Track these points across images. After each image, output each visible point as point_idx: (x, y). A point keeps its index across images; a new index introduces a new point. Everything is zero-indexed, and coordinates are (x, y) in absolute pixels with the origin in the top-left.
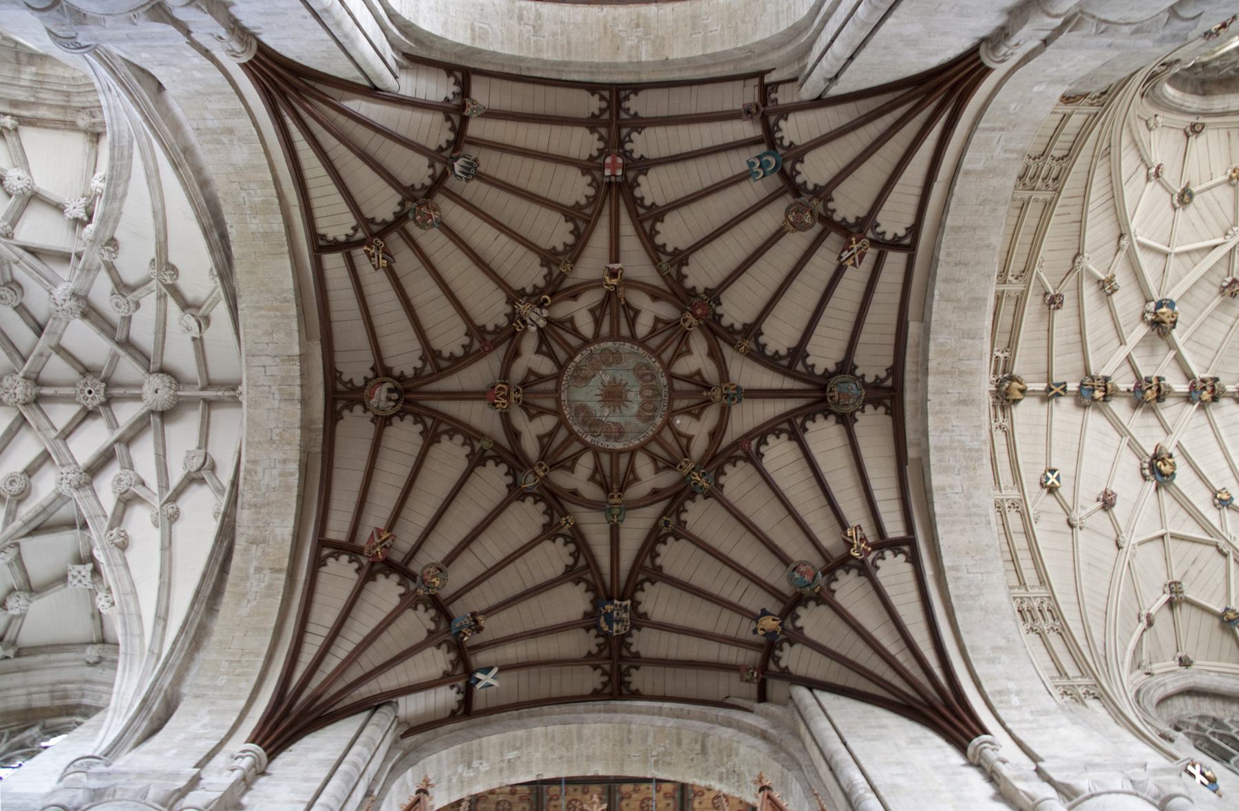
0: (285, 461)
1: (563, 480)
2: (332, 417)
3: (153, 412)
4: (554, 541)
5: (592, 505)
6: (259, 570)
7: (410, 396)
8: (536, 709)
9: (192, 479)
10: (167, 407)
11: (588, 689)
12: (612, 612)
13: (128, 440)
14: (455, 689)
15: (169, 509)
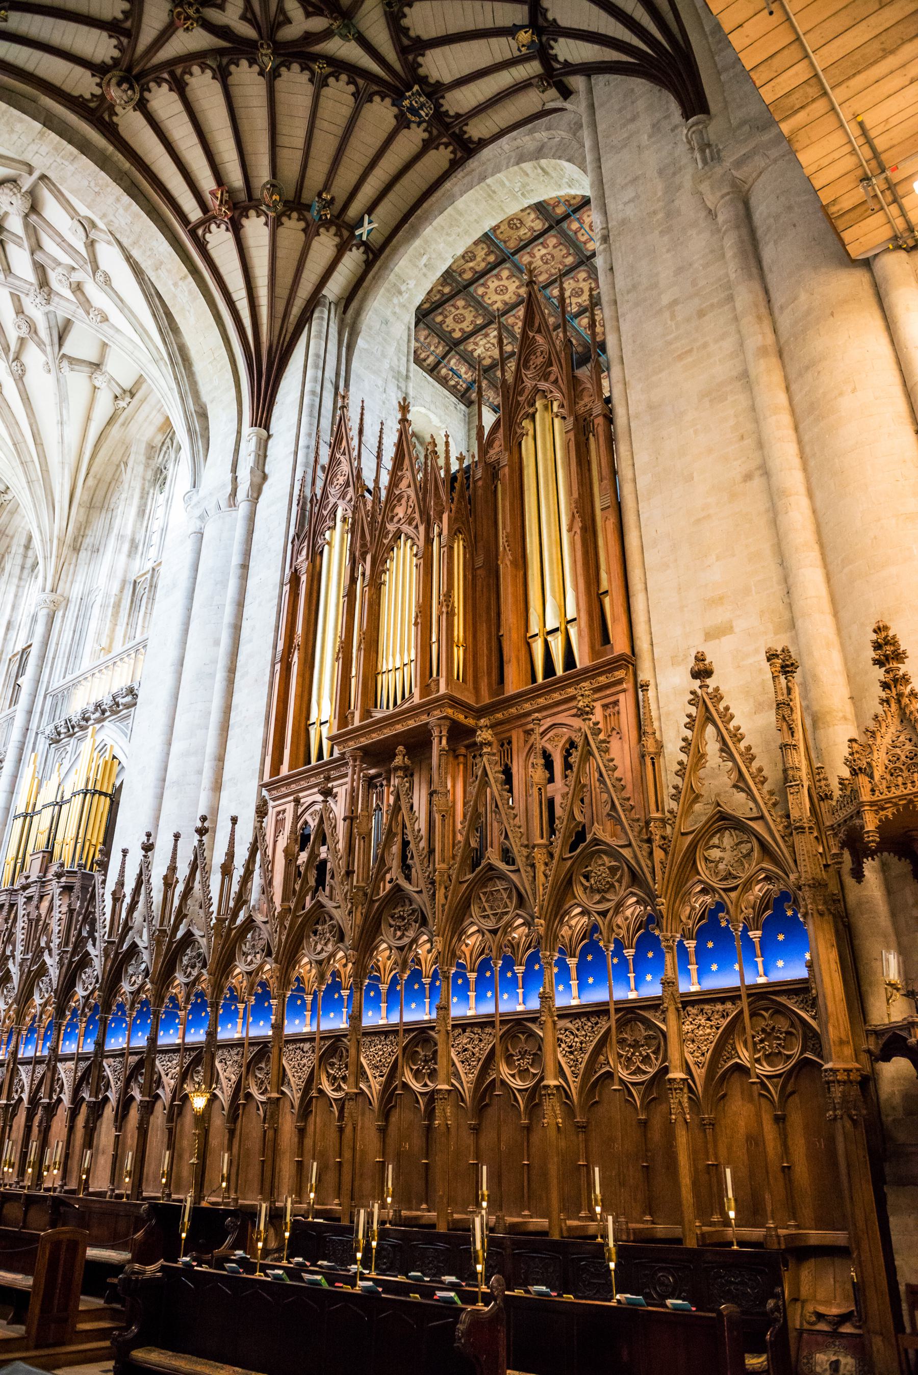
0: (118, 200)
1: (290, 33)
2: (111, 131)
3: (27, 215)
4: (327, 85)
5: (327, 34)
6: (175, 285)
7: (136, 71)
8: (419, 212)
9: (91, 245)
10: (28, 205)
11: (446, 165)
12: (411, 104)
13: (37, 247)
14: (354, 249)
15: (100, 278)
